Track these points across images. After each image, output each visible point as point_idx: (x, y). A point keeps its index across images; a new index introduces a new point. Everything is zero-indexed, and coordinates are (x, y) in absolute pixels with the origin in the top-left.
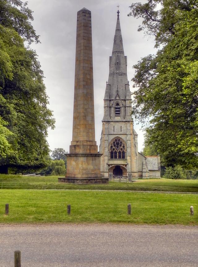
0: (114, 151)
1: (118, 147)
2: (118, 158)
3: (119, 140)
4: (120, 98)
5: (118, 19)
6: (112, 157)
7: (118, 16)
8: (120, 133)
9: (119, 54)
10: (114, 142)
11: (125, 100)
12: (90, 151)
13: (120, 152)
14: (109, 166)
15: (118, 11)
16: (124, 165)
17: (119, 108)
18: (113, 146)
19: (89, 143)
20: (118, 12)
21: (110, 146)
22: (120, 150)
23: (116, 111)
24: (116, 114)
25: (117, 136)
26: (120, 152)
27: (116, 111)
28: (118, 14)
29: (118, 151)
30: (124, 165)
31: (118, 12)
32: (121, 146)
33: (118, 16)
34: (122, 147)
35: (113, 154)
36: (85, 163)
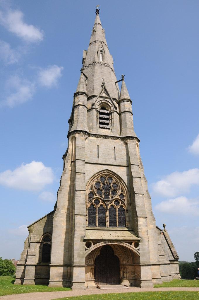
6: (91, 222)
10: (98, 183)
13: (112, 210)
14: (88, 245)
16: (131, 244)
18: (95, 191)
22: (113, 204)
24: (100, 123)
29: (107, 206)
30: (130, 242)
32: (115, 192)
34: (117, 197)
35: (95, 213)
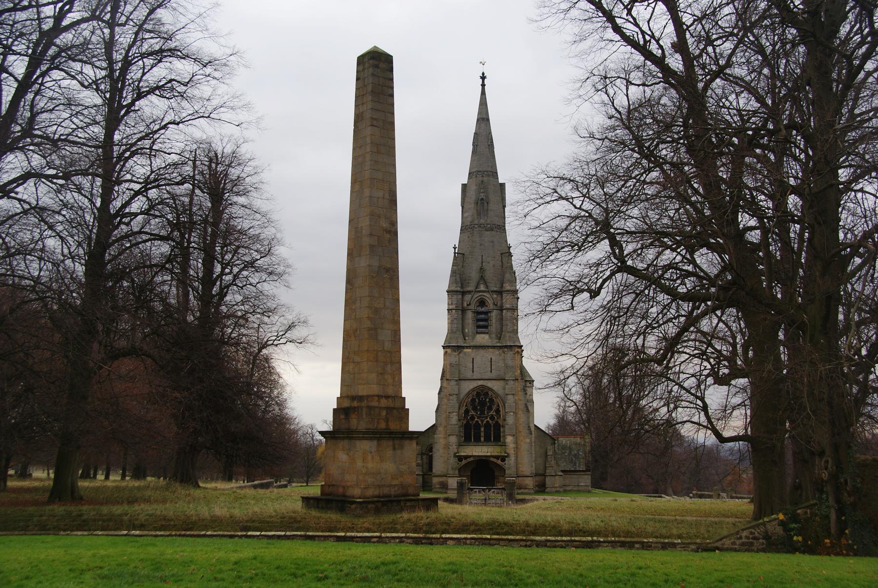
0: (474, 422)
1: (482, 412)
2: (482, 439)
3: (487, 394)
4: (487, 287)
5: (483, 93)
7: (483, 85)
8: (488, 375)
9: (485, 179)
10: (473, 400)
11: (500, 293)
12: (387, 425)
15: (483, 74)
17: (486, 313)
19: (384, 402)
20: (483, 78)
21: (464, 408)
22: (488, 419)
23: (478, 320)
24: (479, 327)
25: (480, 383)
26: (487, 426)
27: (478, 320)
28: (483, 81)
29: (482, 421)
30: (497, 457)
31: (483, 78)
32: (490, 408)
33: (483, 85)
34: (492, 413)
36: (373, 458)
